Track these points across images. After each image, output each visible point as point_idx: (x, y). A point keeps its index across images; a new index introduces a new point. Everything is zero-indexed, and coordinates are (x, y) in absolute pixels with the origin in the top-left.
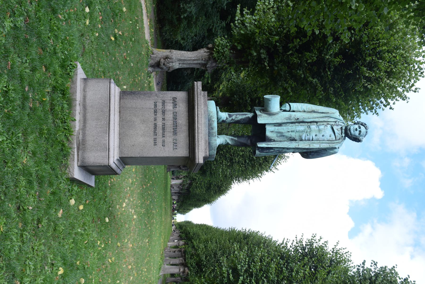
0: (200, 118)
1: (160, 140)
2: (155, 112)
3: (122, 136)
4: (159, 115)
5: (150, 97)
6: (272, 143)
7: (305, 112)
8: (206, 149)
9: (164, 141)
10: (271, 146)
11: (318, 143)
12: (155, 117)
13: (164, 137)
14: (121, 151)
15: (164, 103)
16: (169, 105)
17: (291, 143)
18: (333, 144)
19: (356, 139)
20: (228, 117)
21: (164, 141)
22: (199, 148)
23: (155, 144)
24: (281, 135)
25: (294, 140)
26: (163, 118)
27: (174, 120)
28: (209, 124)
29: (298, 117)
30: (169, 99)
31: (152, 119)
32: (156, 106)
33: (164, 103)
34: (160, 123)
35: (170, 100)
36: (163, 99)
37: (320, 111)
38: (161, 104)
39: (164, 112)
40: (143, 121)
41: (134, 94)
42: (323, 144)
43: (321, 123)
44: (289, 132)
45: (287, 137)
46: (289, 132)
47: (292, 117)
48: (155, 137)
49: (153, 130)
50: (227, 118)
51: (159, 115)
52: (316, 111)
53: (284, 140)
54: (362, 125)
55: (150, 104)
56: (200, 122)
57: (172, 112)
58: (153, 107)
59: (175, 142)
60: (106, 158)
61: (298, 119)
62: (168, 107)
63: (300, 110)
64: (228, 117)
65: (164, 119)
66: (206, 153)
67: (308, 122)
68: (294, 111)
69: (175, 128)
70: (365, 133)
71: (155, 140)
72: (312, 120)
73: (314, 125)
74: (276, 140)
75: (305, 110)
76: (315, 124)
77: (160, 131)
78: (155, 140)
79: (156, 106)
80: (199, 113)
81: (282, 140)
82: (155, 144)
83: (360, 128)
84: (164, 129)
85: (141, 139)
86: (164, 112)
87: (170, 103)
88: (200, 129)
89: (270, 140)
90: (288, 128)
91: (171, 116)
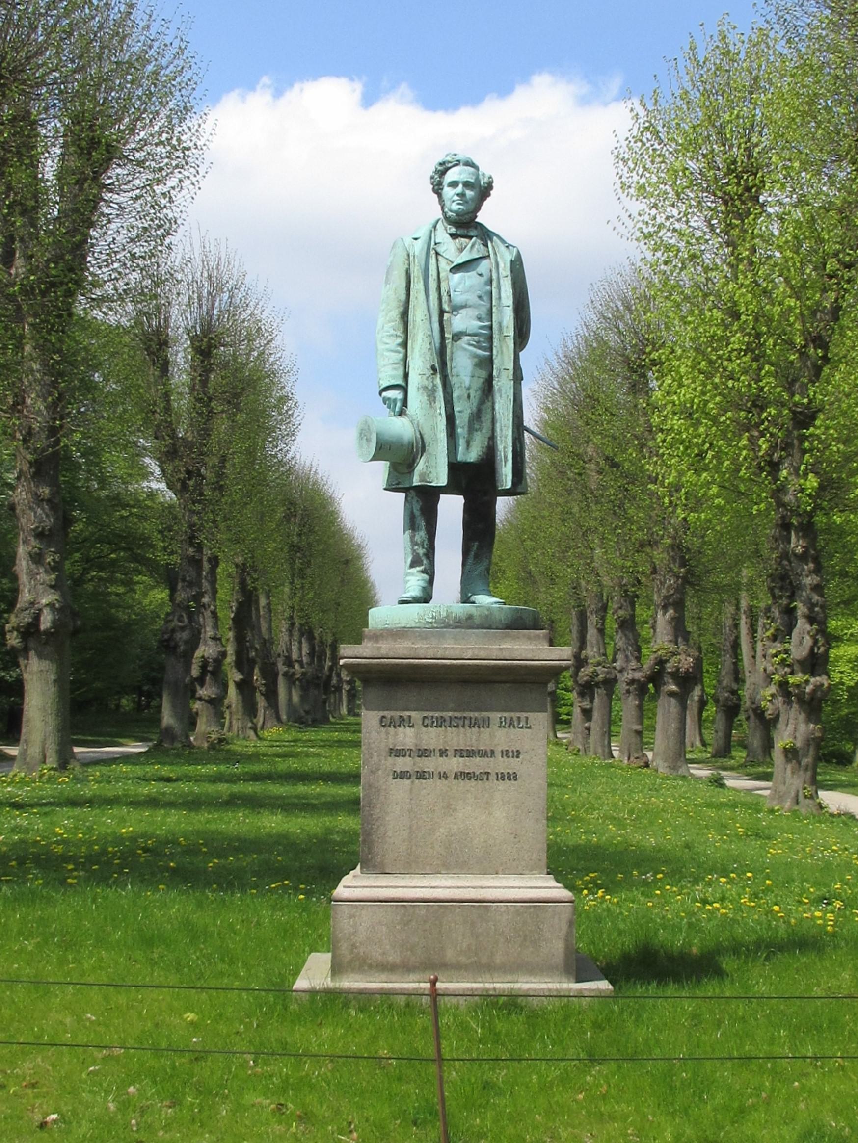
0: (447, 654)
1: (501, 764)
2: (422, 775)
3: (488, 864)
4: (429, 764)
5: (379, 791)
6: (500, 447)
7: (405, 345)
8: (529, 638)
9: (506, 754)
10: (510, 449)
11: (501, 312)
12: (436, 777)
13: (492, 752)
14: (532, 869)
15: (397, 753)
16: (401, 737)
17: (500, 390)
18: (501, 265)
19: (484, 191)
20: (422, 568)
21: (506, 754)
22: (529, 656)
23: (512, 777)
24: (476, 417)
25: (489, 382)
26: (441, 756)
27: (447, 723)
28: (456, 627)
29: (428, 366)
30: (383, 735)
31: (441, 784)
32: (403, 775)
33: (397, 753)
34: (455, 764)
35: (387, 733)
36: (384, 753)
37: (403, 297)
38: (400, 760)
39: (424, 753)
40: (449, 809)
41: (369, 835)
42: (503, 295)
43: (445, 298)
44: (469, 396)
45: (482, 402)
46: (469, 396)
47: (426, 383)
48: (493, 777)
49: (473, 782)
50: (423, 572)
51: (429, 764)
52: (402, 309)
53: (489, 410)
54: (443, 173)
55: (399, 790)
56: (457, 654)
57: (424, 729)
58: (407, 782)
59: (508, 721)
60: (459, 907)
61: (433, 368)
62: (408, 740)
63: (401, 356)
64: (422, 568)
65: (443, 753)
66: (538, 636)
67: (443, 338)
68: (406, 376)
69: (467, 722)
70: (472, 169)
71: (501, 777)
72: (436, 326)
73: (449, 320)
74: (489, 435)
75: (400, 340)
76: (446, 316)
77: (476, 764)
78: (501, 777)
79: (403, 775)
80: (430, 654)
81: (489, 416)
82: (512, 777)
83: (454, 184)
84: (470, 754)
85: (499, 814)
86: (424, 753)
87: (396, 734)
88: (476, 653)
89: (490, 452)
90: (459, 398)
91: (433, 731)
